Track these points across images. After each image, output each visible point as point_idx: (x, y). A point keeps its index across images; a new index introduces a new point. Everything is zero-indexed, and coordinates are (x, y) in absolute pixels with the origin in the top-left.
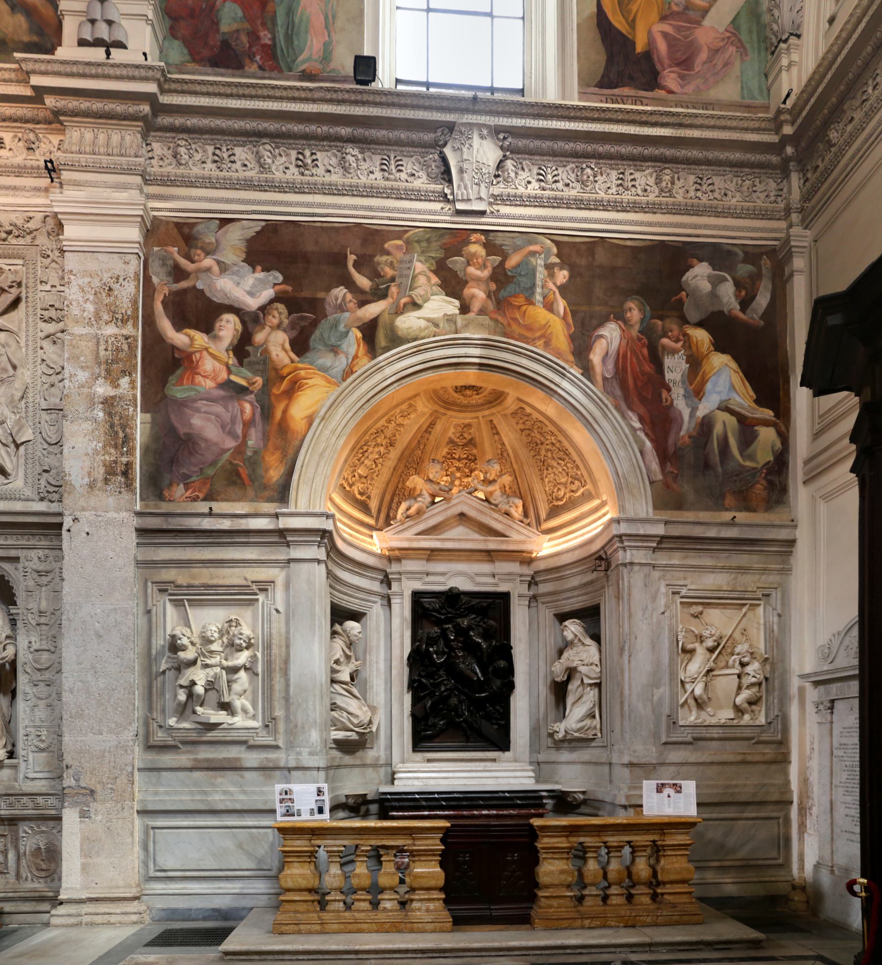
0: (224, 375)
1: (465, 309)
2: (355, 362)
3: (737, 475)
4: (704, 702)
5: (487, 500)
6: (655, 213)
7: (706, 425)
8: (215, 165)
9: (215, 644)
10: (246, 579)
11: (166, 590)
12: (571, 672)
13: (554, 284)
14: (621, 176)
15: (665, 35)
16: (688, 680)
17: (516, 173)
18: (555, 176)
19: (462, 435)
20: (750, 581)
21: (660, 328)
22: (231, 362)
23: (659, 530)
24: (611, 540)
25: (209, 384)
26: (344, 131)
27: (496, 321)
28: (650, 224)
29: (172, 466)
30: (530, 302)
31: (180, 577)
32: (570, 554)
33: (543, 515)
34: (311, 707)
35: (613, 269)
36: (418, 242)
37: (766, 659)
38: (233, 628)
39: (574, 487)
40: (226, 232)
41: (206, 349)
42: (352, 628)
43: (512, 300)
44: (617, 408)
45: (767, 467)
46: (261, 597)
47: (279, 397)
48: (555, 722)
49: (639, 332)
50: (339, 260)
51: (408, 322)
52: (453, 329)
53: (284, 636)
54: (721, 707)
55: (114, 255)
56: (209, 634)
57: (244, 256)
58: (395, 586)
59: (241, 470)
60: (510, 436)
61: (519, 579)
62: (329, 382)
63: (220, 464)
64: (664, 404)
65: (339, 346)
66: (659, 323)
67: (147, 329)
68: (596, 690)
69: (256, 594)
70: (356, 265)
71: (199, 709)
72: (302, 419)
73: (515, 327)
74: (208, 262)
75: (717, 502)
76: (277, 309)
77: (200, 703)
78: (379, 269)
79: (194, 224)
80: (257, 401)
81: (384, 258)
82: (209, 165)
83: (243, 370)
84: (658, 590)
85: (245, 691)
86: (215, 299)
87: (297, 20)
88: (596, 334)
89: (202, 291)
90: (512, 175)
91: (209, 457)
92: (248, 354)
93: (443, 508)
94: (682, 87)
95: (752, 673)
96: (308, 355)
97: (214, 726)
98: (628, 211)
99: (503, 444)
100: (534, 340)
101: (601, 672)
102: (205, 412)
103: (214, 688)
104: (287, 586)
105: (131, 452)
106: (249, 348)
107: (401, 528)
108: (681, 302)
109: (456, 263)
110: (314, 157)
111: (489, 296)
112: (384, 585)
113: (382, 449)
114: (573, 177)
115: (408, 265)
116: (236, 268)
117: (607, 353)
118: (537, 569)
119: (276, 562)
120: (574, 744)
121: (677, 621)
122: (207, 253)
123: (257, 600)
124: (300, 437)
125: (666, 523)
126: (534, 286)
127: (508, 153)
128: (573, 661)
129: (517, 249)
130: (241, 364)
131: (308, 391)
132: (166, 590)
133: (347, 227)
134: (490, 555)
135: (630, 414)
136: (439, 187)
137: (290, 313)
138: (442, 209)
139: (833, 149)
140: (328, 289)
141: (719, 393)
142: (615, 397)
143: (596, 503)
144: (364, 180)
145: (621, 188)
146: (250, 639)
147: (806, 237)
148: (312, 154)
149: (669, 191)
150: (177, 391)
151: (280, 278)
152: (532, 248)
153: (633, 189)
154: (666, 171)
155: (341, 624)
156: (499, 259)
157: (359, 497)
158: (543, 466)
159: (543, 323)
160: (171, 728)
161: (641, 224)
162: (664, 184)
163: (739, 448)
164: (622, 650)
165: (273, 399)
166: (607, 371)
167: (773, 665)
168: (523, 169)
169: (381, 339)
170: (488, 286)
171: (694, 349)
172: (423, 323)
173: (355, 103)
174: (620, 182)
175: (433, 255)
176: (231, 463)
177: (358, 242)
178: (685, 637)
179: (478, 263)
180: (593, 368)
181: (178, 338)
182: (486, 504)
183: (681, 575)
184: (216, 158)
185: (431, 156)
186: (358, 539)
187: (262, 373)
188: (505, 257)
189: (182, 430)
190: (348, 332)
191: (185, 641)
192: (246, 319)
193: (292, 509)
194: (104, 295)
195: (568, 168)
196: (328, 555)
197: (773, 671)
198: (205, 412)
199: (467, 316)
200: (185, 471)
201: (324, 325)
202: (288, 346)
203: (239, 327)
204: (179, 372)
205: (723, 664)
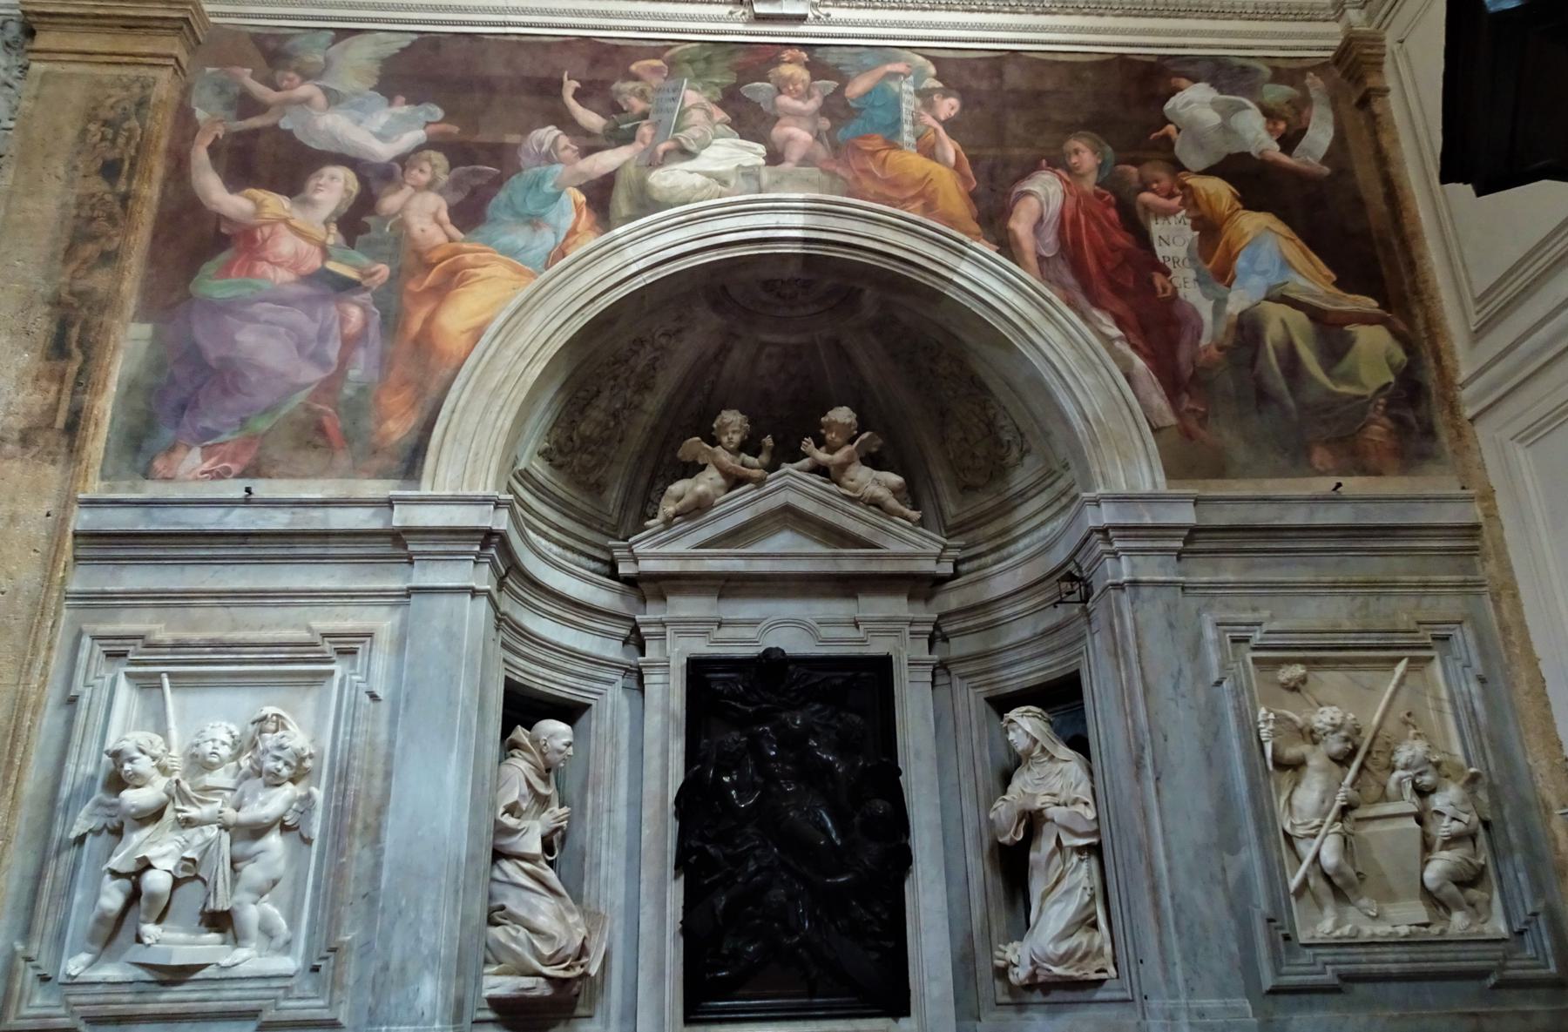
0: (314, 262)
1: (774, 157)
2: (570, 240)
3: (1327, 411)
4: (1350, 884)
6: (1102, 15)
7: (1248, 329)
9: (220, 771)
10: (310, 629)
11: (124, 654)
12: (1033, 821)
13: (935, 118)
16: (1300, 831)
20: (1401, 611)
22: (331, 241)
23: (1186, 515)
24: (1086, 540)
25: (284, 275)
27: (833, 175)
28: (1096, 31)
29: (183, 413)
30: (892, 144)
31: (159, 627)
34: (427, 916)
35: (1038, 95)
36: (690, 62)
37: (1474, 778)
38: (267, 735)
40: (346, 48)
41: (286, 221)
43: (860, 143)
44: (1071, 304)
45: (1384, 393)
46: (338, 668)
47: (418, 298)
48: (1009, 939)
49: (1097, 184)
50: (549, 88)
52: (755, 186)
53: (382, 750)
54: (1389, 895)
57: (375, 82)
59: (327, 421)
62: (520, 271)
63: (284, 411)
64: (1161, 295)
65: (541, 216)
66: (1133, 170)
67: (171, 186)
68: (1094, 863)
70: (578, 95)
71: (150, 930)
72: (463, 332)
73: (867, 183)
74: (305, 90)
75: (1297, 459)
76: (429, 160)
77: (156, 916)
78: (620, 101)
79: (287, 37)
80: (375, 304)
81: (630, 85)
83: (354, 253)
84: (1199, 636)
85: (275, 883)
86: (313, 145)
88: (1018, 189)
89: (289, 133)
91: (264, 399)
92: (366, 229)
95: (1449, 810)
96: (481, 228)
97: (178, 975)
98: (1055, 13)
100: (904, 201)
101: (1097, 819)
102: (266, 322)
103: (196, 877)
104: (401, 642)
106: (369, 220)
108: (1168, 142)
109: (759, 90)
111: (818, 138)
115: (671, 95)
116: (356, 100)
117: (1041, 220)
119: (382, 594)
120: (1056, 996)
121: (1252, 699)
122: (306, 77)
123: (331, 673)
124: (454, 363)
125: (1197, 501)
126: (897, 122)
128: (1034, 796)
129: (864, 69)
130: (351, 243)
131: (479, 288)
133: (565, 43)
135: (1097, 313)
137: (453, 165)
138: (731, 13)
140: (526, 130)
141: (1264, 273)
146: (301, 760)
150: (213, 284)
151: (439, 113)
152: (890, 68)
156: (836, 84)
159: (919, 175)
160: (73, 982)
161: (1081, 30)
163: (1322, 364)
164: (1138, 764)
165: (407, 300)
166: (1045, 247)
167: (1492, 790)
169: (621, 202)
170: (816, 123)
171: (1204, 207)
172: (699, 180)
175: (717, 81)
176: (307, 409)
177: (584, 63)
178: (1274, 733)
179: (797, 91)
180: (1017, 243)
183: (1246, 601)
187: (390, 258)
188: (844, 80)
189: (213, 353)
190: (558, 196)
191: (144, 765)
192: (369, 174)
197: (1496, 803)
198: (266, 322)
199: (779, 168)
200: (208, 423)
201: (516, 182)
202: (444, 215)
203: (354, 186)
204: (224, 257)
205: (1374, 791)
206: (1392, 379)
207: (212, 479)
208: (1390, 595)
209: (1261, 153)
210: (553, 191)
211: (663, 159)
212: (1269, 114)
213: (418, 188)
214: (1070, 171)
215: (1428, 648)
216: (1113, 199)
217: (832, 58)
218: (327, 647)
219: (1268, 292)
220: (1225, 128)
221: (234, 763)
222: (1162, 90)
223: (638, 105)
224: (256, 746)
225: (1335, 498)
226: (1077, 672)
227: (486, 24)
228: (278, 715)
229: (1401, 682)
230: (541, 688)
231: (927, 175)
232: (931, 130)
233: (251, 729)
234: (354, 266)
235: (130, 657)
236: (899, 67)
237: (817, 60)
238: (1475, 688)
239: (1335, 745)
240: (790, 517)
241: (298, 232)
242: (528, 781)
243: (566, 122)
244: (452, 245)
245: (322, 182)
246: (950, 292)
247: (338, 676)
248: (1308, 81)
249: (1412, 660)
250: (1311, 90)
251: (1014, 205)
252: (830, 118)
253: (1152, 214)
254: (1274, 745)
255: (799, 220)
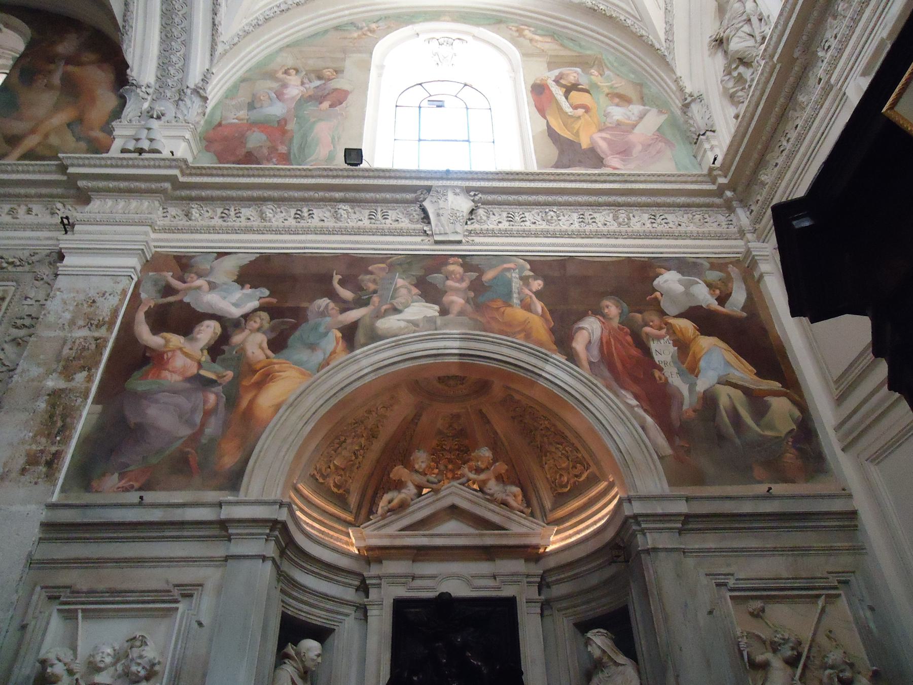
0: (193, 370)
1: (444, 312)
2: (332, 356)
5: (481, 490)
6: (617, 238)
8: (221, 219)
9: (104, 673)
10: (167, 582)
13: (531, 290)
14: (581, 216)
15: (604, 139)
17: (488, 217)
18: (522, 217)
19: (450, 426)
21: (640, 320)
22: (203, 359)
26: (337, 195)
30: (508, 304)
32: (582, 547)
33: (548, 504)
36: (400, 264)
39: (576, 472)
41: (181, 349)
42: (308, 650)
51: (385, 324)
55: (106, 277)
56: (98, 658)
57: (235, 278)
58: (373, 594)
60: (501, 425)
61: (525, 580)
62: (303, 374)
66: (638, 316)
69: (176, 601)
76: (260, 317)
79: (193, 257)
81: (368, 277)
82: (216, 219)
86: (198, 310)
87: (309, 139)
88: (576, 326)
89: (188, 304)
90: (484, 218)
92: (223, 352)
93: (431, 500)
94: (624, 165)
99: (496, 433)
100: (515, 333)
104: (220, 590)
105: (66, 441)
106: (225, 348)
107: (382, 523)
108: (657, 301)
109: (436, 278)
110: (311, 212)
111: (467, 301)
112: (362, 594)
113: (363, 441)
114: (539, 218)
116: (225, 286)
117: (590, 342)
118: (548, 568)
119: (211, 559)
122: (200, 276)
126: (509, 294)
127: (479, 204)
129: (492, 267)
132: (59, 597)
134: (489, 553)
136: (419, 226)
137: (272, 319)
138: (422, 240)
139: (767, 186)
140: (312, 300)
142: (603, 378)
143: (603, 485)
144: (351, 224)
145: (582, 223)
147: (766, 248)
148: (309, 210)
149: (627, 224)
150: (139, 383)
151: (267, 292)
152: (506, 266)
153: (594, 224)
154: (620, 211)
155: (296, 643)
157: (335, 490)
158: (541, 452)
162: (621, 220)
168: (494, 214)
169: (360, 336)
172: (403, 324)
173: (348, 177)
174: (581, 220)
180: (577, 355)
181: (154, 340)
182: (479, 494)
184: (224, 215)
185: (412, 208)
186: (332, 537)
188: (480, 271)
189: (133, 419)
190: (326, 334)
193: (242, 496)
194: (85, 305)
195: (533, 212)
196: (282, 553)
199: (446, 317)
201: (304, 327)
202: (265, 345)
206: (795, 427)
207: (123, 491)
208: (808, 555)
209: (707, 306)
210: (325, 331)
211: (384, 314)
212: (709, 285)
213: (252, 331)
214: (604, 316)
215: (835, 588)
216: (629, 330)
217: (475, 261)
218: (176, 593)
219: (719, 379)
220: (687, 293)
221: (114, 668)
222: (651, 274)
223: (372, 287)
224: (128, 656)
225: (769, 496)
226: (627, 605)
227: (294, 248)
228: (142, 636)
229: (823, 610)
230: (304, 619)
231: (525, 321)
232: (528, 297)
233: (126, 645)
234: (215, 372)
235: (62, 599)
236: (511, 265)
237: (467, 262)
238: (868, 614)
239: (788, 652)
240: (454, 511)
241: (186, 354)
242: (292, 679)
243: (332, 295)
244: (269, 360)
245: (202, 328)
246: (541, 382)
247: (180, 611)
248: (729, 269)
249: (828, 596)
250: (732, 274)
251: (575, 334)
252: (474, 291)
253: (651, 339)
254: (747, 652)
255: (457, 344)
